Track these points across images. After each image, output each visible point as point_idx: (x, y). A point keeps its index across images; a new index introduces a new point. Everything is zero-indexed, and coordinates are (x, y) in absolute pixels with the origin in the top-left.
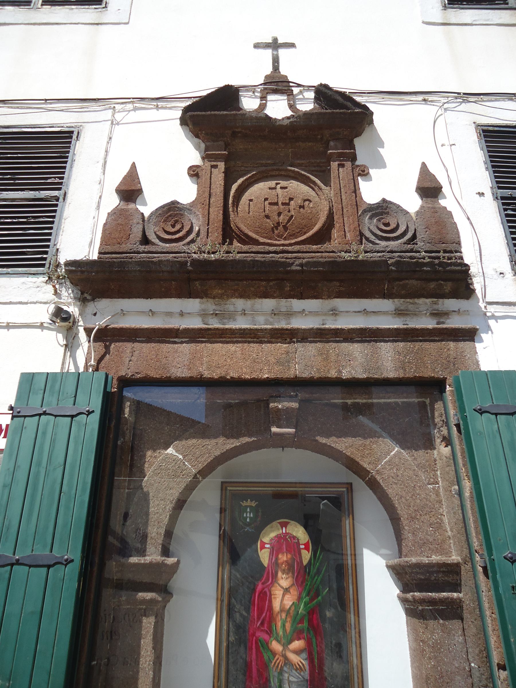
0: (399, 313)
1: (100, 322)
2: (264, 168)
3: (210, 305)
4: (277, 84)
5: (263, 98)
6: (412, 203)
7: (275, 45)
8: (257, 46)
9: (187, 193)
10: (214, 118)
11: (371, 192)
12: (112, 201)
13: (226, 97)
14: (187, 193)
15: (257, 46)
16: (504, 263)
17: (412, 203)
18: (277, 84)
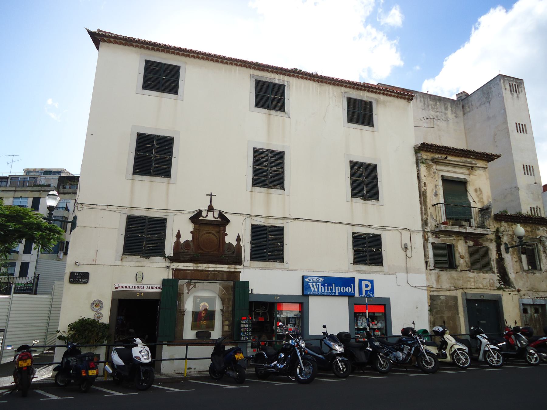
0: (228, 268)
1: (174, 267)
2: (206, 232)
3: (195, 265)
4: (211, 208)
5: (207, 213)
6: (235, 243)
7: (211, 195)
8: (207, 195)
9: (190, 237)
10: (196, 218)
11: (228, 240)
12: (175, 239)
13: (200, 213)
14: (190, 237)
15: (207, 195)
16: (249, 259)
17: (235, 243)
18: (211, 208)
